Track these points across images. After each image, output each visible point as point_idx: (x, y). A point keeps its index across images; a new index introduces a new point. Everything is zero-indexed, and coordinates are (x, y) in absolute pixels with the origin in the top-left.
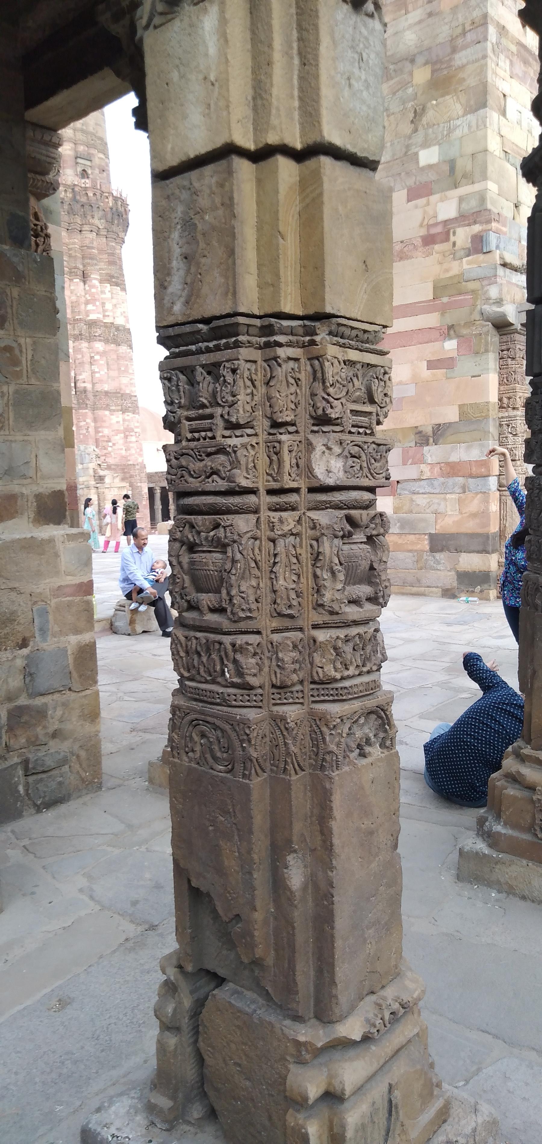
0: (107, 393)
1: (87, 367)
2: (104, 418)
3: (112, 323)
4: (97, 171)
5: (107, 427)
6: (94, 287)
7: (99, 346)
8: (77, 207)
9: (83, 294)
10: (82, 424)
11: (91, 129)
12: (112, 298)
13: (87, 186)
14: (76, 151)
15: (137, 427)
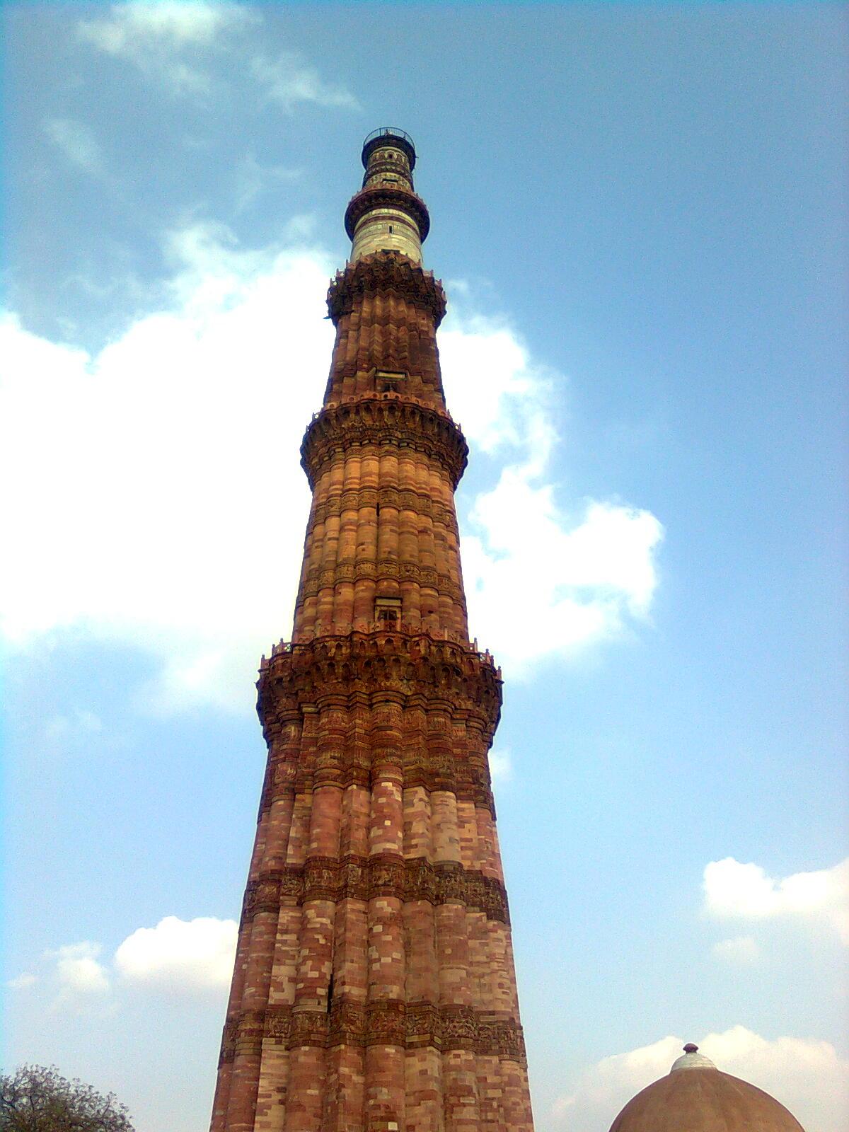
0: (393, 1005)
1: (354, 952)
2: (382, 1063)
3: (423, 859)
4: (416, 613)
5: (387, 1085)
6: (385, 793)
7: (385, 905)
8: (356, 667)
9: (364, 810)
10: (334, 1077)
11: (407, 557)
12: (433, 813)
13: (378, 630)
14: (376, 590)
15: (494, 1086)
